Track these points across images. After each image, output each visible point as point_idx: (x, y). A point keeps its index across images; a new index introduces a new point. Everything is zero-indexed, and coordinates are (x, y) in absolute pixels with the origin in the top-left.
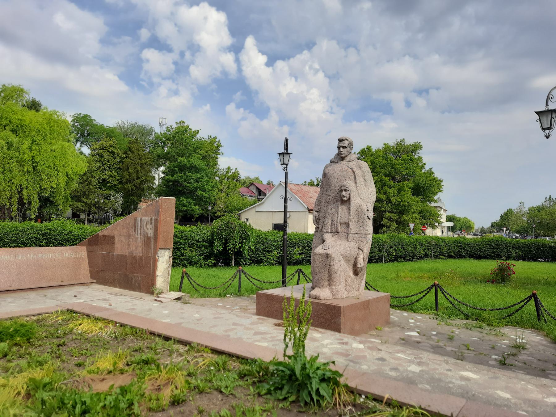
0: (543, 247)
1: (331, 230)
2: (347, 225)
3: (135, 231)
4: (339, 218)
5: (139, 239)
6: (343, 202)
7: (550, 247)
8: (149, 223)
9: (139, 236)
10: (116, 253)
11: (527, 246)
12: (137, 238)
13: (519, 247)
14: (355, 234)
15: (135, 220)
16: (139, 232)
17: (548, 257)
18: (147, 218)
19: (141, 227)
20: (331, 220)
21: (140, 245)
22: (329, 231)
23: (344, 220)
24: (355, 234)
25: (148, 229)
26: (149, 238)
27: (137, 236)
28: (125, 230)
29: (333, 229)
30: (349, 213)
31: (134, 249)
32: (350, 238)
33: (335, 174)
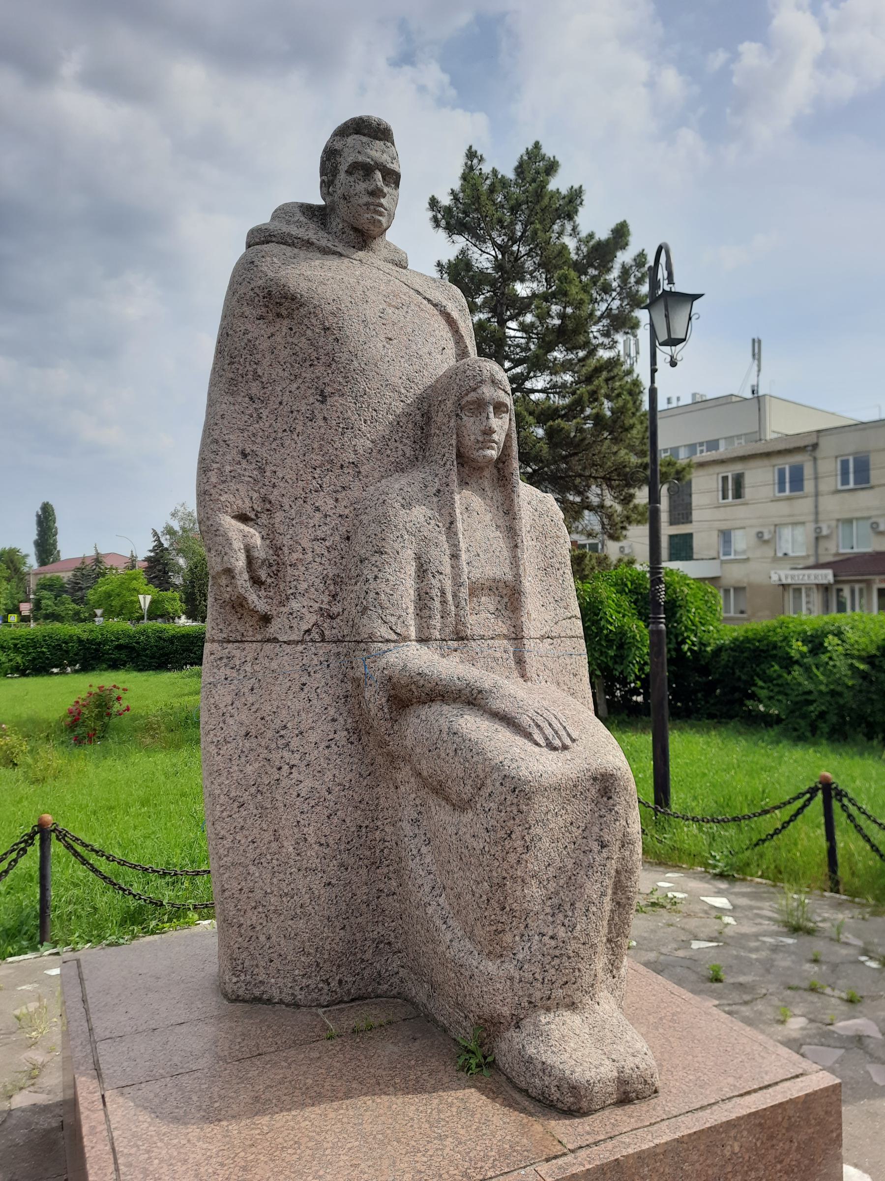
0: (66, 643)
1: (420, 629)
2: (510, 597)
4: (464, 556)
6: (467, 466)
7: (80, 641)
11: (33, 643)
13: (15, 645)
14: (542, 638)
17: (72, 663)
20: (411, 569)
22: (413, 632)
23: (500, 570)
24: (542, 638)
29: (437, 622)
30: (512, 532)
32: (533, 663)
33: (371, 313)
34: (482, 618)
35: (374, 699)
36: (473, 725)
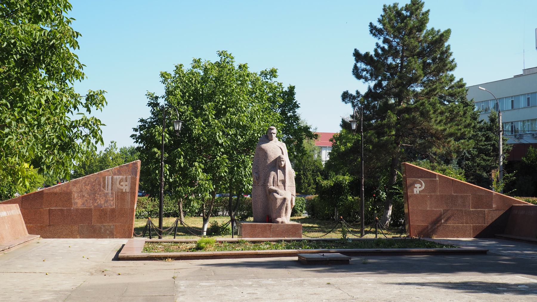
2: (284, 182)
3: (104, 187)
5: (110, 194)
8: (124, 180)
9: (110, 192)
10: (74, 207)
12: (107, 193)
15: (104, 179)
16: (110, 187)
18: (121, 177)
19: (112, 184)
21: (111, 199)
25: (122, 185)
26: (123, 193)
27: (106, 192)
28: (88, 187)
31: (103, 202)
34: (280, 184)
35: (268, 191)
36: (275, 194)
